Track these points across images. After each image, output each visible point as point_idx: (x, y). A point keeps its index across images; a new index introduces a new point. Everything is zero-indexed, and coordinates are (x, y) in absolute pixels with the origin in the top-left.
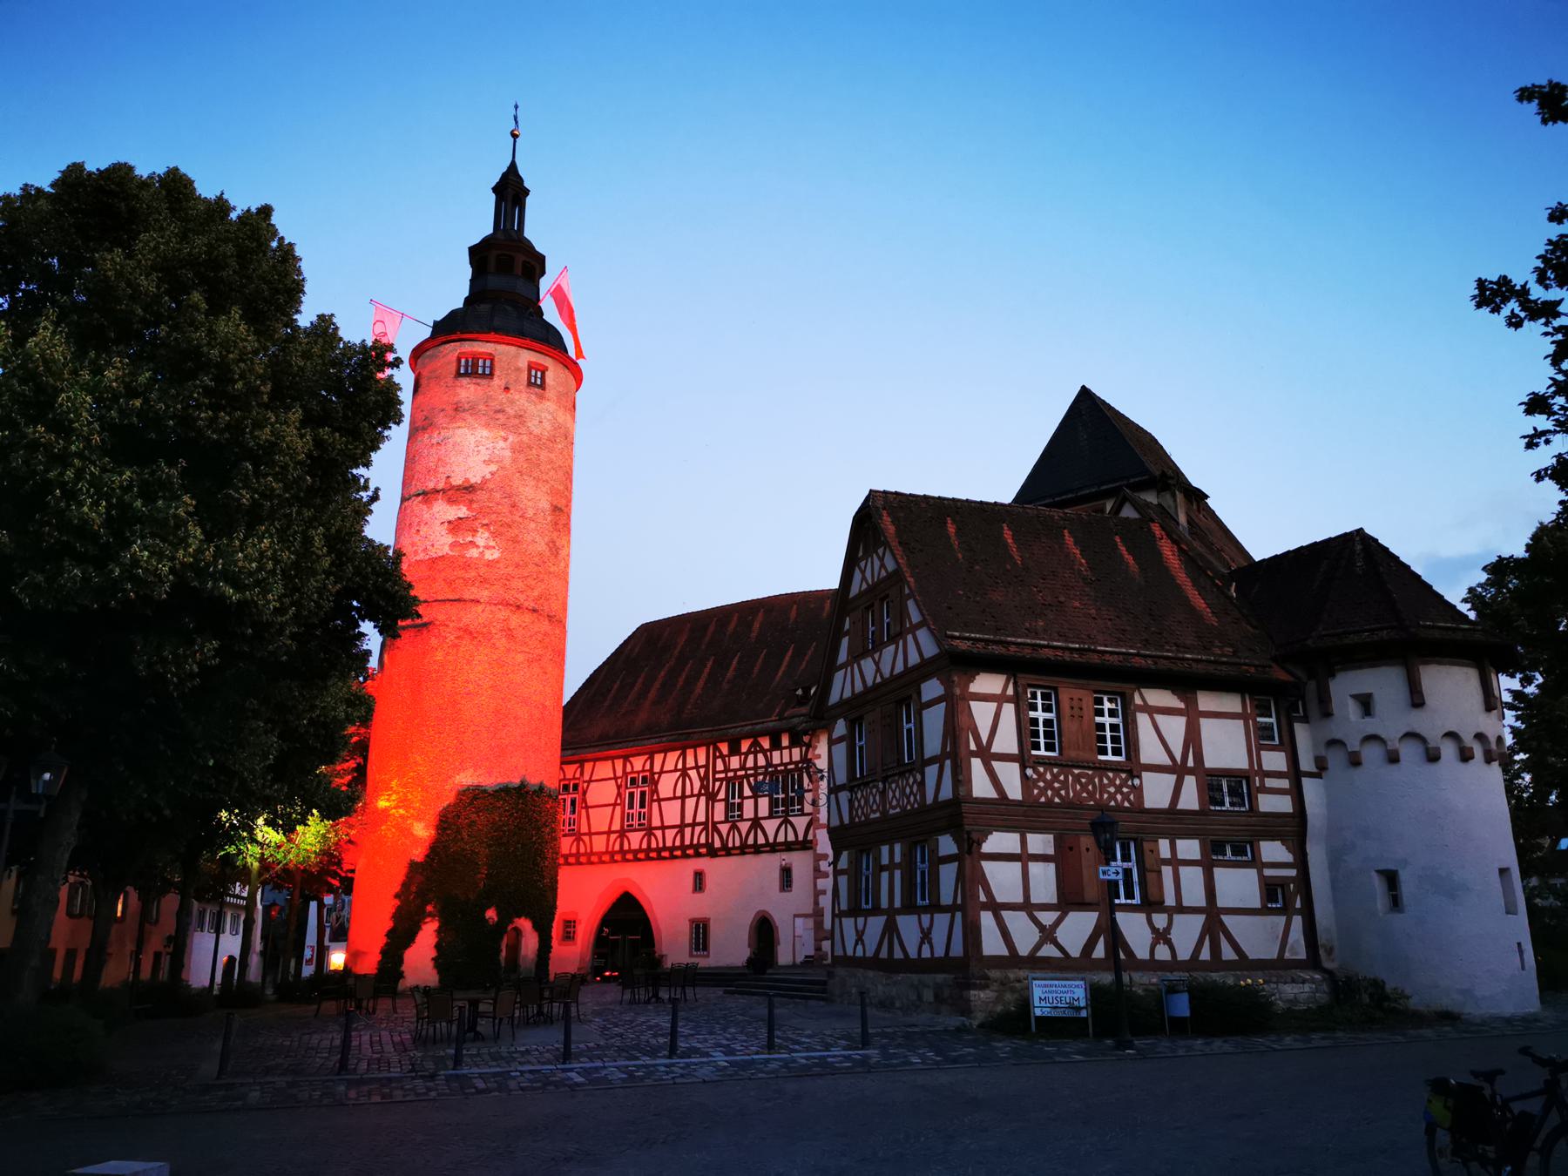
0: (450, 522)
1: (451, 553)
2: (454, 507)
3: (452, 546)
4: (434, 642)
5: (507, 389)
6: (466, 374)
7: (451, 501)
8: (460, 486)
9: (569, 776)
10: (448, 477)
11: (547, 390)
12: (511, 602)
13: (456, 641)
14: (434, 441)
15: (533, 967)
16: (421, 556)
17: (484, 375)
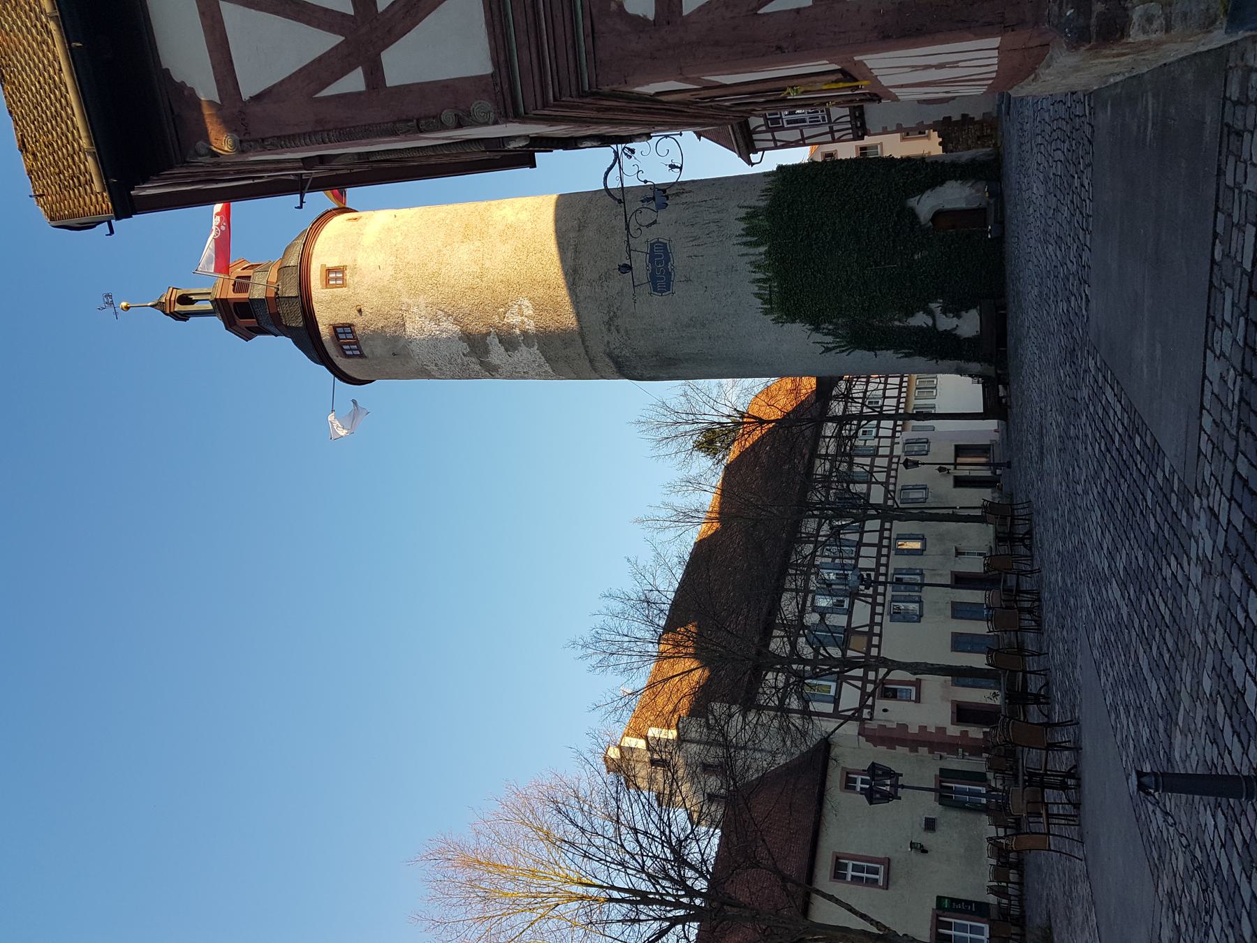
0: (507, 350)
1: (536, 347)
2: (490, 348)
3: (529, 346)
4: (626, 352)
5: (360, 311)
6: (359, 349)
7: (487, 352)
8: (469, 344)
9: (761, 121)
10: (464, 354)
11: (345, 264)
12: (571, 280)
13: (622, 332)
14: (436, 368)
15: (981, 185)
16: (547, 368)
17: (352, 332)
